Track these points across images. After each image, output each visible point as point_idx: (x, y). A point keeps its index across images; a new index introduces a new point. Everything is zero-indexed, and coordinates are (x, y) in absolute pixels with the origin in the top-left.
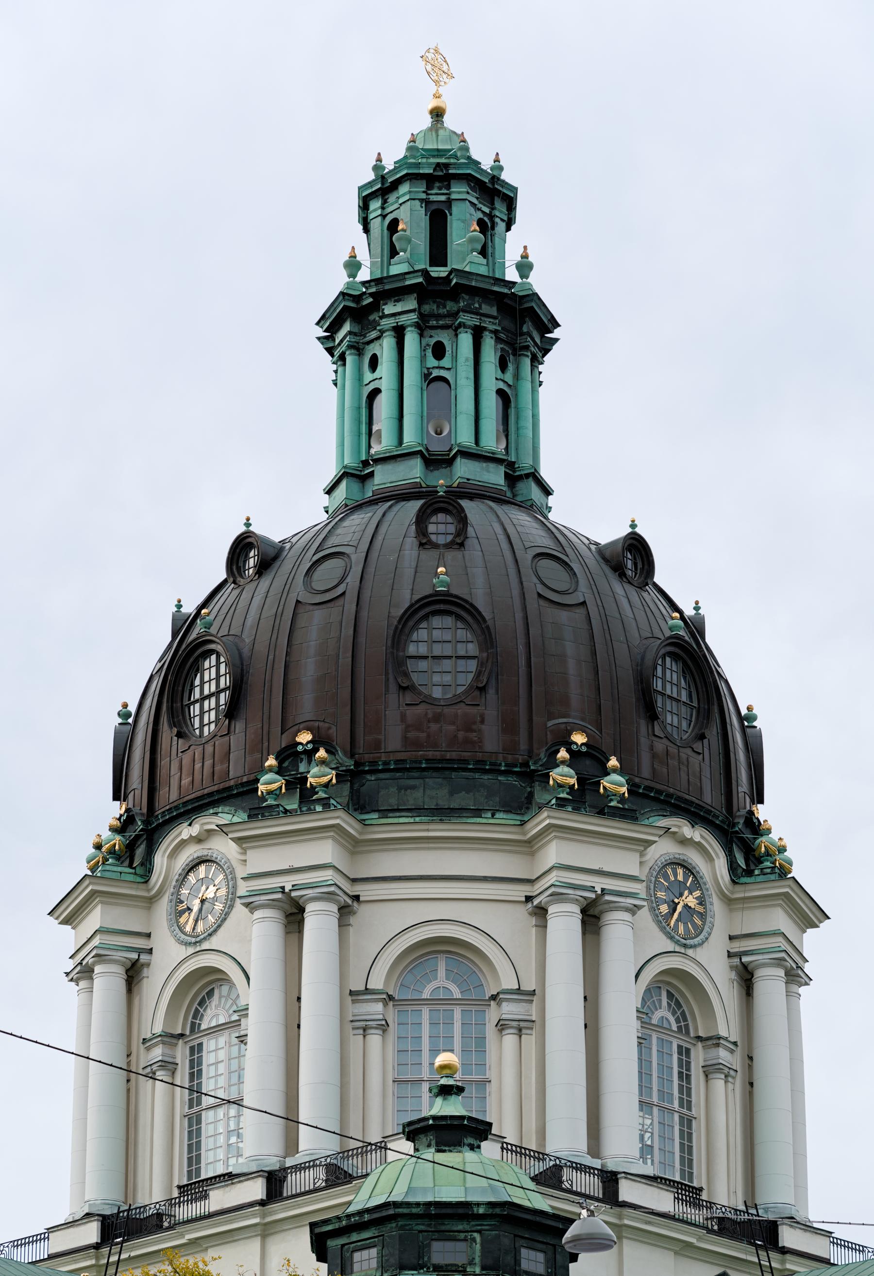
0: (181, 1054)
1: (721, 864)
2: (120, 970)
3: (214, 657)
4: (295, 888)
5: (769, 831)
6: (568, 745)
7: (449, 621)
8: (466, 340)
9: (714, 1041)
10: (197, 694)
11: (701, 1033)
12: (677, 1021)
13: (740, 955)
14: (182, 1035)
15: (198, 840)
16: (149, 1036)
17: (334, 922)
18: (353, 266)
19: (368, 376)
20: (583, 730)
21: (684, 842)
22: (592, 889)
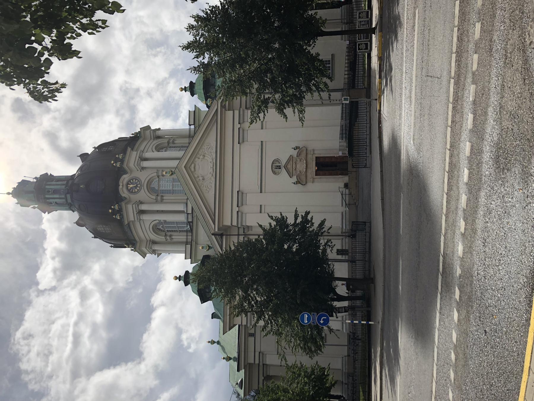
0: (169, 234)
3: (97, 228)
4: (136, 212)
5: (133, 134)
6: (113, 163)
8: (47, 187)
9: (168, 143)
10: (104, 231)
13: (154, 138)
16: (165, 240)
17: (143, 205)
18: (34, 208)
19: (53, 204)
20: (111, 161)
22: (138, 159)
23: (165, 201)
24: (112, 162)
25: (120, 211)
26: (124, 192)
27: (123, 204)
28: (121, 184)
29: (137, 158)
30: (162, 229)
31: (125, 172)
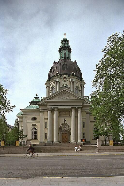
24: (72, 72)
26: (63, 77)
28: (65, 75)
29: (73, 80)
31: (69, 76)
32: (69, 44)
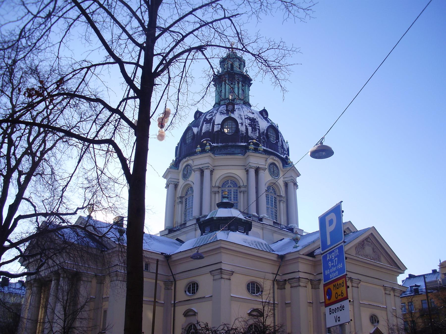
1: (281, 165)
2: (173, 185)
7: (231, 121)
9: (281, 196)
11: (278, 195)
12: (274, 192)
14: (184, 197)
15: (186, 161)
21: (275, 160)
23: (213, 195)
25: (203, 151)
27: (210, 154)
30: (188, 193)
32: (244, 66)
